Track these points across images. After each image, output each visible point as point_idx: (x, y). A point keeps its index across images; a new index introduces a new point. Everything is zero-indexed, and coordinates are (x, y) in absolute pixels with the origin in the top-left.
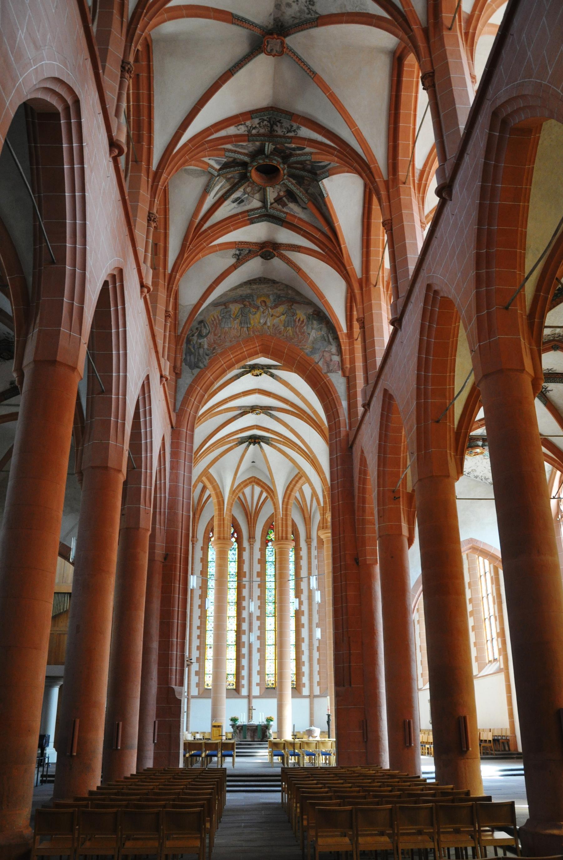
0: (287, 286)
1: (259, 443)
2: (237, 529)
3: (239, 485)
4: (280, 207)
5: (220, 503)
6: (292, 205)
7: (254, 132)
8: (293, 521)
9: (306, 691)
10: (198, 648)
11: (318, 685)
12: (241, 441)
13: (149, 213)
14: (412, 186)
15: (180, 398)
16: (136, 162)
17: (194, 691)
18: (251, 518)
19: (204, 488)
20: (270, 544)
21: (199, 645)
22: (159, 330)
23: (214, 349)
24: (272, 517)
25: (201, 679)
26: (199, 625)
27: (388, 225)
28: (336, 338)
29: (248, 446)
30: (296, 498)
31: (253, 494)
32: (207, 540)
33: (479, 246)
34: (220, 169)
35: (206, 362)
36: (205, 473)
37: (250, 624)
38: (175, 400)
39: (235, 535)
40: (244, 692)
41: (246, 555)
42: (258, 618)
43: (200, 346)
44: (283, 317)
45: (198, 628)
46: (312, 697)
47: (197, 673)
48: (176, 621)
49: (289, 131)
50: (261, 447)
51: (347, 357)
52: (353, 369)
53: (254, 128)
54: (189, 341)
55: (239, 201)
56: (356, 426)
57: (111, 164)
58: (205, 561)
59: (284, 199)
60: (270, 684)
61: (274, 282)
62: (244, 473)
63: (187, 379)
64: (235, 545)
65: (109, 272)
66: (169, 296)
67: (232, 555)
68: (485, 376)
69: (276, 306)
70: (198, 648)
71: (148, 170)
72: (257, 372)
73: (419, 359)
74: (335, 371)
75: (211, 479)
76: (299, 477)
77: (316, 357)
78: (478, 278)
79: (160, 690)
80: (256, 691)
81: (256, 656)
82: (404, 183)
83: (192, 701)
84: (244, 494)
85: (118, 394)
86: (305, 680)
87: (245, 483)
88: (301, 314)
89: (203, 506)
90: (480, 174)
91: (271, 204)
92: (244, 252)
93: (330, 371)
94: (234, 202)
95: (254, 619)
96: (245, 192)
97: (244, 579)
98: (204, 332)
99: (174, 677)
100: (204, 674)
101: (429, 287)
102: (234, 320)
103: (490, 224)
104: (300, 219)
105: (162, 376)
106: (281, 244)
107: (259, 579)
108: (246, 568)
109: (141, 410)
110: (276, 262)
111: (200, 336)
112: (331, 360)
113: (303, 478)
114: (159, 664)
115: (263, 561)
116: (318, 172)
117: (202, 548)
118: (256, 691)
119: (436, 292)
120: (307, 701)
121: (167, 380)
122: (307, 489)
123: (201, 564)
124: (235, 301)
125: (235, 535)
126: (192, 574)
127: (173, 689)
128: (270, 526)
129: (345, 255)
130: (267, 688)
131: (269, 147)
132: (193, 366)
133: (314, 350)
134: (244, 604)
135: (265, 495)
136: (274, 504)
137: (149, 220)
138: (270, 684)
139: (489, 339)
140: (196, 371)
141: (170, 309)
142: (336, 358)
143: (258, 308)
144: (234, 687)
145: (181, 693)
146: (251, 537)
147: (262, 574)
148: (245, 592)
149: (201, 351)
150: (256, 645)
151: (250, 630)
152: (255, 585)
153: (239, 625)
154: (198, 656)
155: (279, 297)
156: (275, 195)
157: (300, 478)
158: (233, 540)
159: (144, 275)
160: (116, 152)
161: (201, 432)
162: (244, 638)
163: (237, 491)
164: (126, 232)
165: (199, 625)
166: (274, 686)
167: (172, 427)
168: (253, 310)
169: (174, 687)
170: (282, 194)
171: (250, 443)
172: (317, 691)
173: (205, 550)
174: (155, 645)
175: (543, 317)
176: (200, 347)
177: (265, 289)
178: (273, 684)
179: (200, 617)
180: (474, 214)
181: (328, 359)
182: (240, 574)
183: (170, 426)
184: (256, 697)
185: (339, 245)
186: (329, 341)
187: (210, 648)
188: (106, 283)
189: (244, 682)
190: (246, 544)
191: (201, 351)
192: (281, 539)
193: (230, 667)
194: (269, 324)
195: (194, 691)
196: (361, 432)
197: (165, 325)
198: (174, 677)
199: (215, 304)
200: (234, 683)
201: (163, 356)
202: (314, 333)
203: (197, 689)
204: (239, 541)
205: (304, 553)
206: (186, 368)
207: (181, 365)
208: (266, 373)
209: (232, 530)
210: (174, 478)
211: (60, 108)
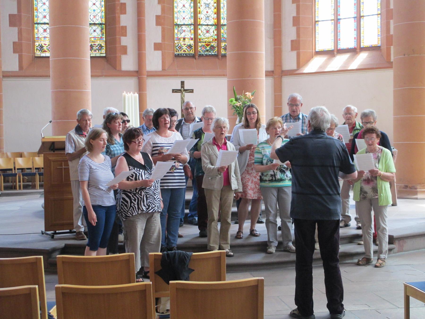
11: (293, 49)
25: (24, 34)
40: (128, 63)
60: (184, 48)
80: (154, 61)
100: (32, 24)
118: (154, 61)
130: (178, 56)
138: (184, 48)
144: (103, 52)
166: (192, 52)
172: (289, 61)
178: (190, 46)
189: (128, 41)
200: (103, 44)
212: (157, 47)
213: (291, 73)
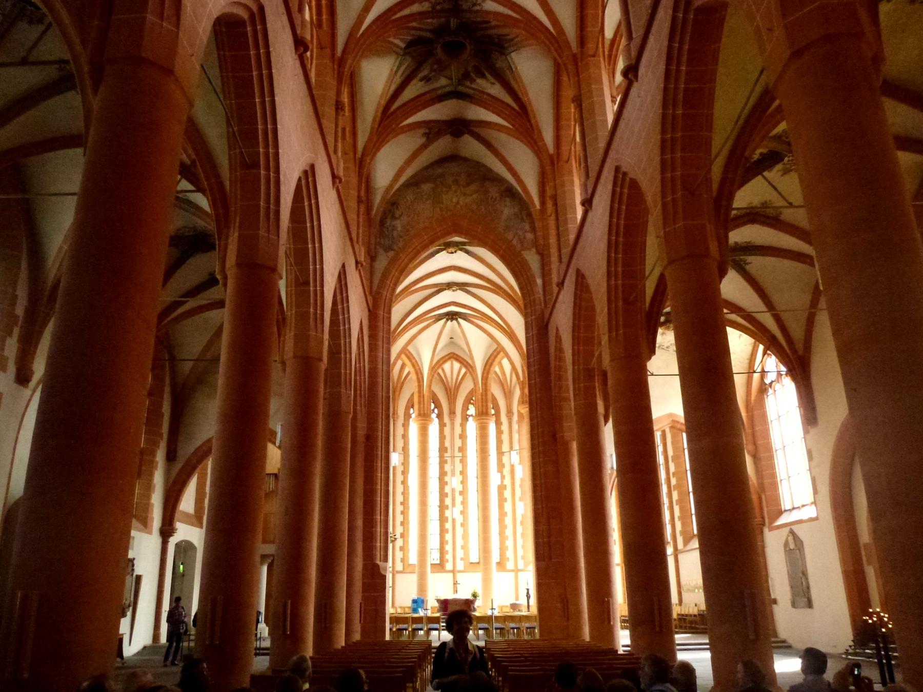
0: (478, 162)
1: (456, 319)
2: (438, 405)
3: (438, 362)
4: (468, 83)
5: (420, 380)
6: (480, 81)
7: (438, 7)
8: (493, 395)
9: (510, 565)
12: (439, 318)
13: (337, 101)
14: (602, 59)
15: (376, 282)
16: (322, 48)
17: (399, 567)
18: (451, 393)
19: (403, 366)
20: (470, 419)
22: (352, 216)
23: (408, 230)
24: (471, 393)
27: (578, 101)
28: (530, 215)
29: (446, 323)
30: (496, 373)
31: (452, 369)
32: (407, 416)
33: (663, 131)
34: (406, 48)
35: (401, 245)
36: (404, 351)
37: (453, 499)
38: (371, 283)
39: (436, 411)
40: (449, 566)
41: (447, 431)
42: (461, 493)
43: (394, 228)
44: (475, 196)
45: (402, 504)
46: (516, 571)
47: (401, 549)
48: (379, 499)
49: (474, 5)
50: (459, 323)
51: (539, 234)
52: (547, 246)
53: (438, 4)
54: (382, 223)
55: (427, 79)
56: (551, 304)
57: (298, 63)
58: (405, 437)
59: (473, 75)
61: (465, 159)
62: (442, 349)
63: (382, 262)
64: (436, 421)
65: (301, 169)
66: (360, 182)
67: (434, 428)
68: (670, 263)
69: (468, 184)
70: (402, 524)
71: (333, 55)
72: (451, 250)
73: (609, 241)
74: (529, 249)
75: (410, 357)
76: (497, 352)
77: (510, 236)
78: (663, 163)
79: (365, 566)
80: (460, 565)
81: (459, 531)
82: (594, 56)
83: (398, 576)
84: (443, 370)
85: (315, 286)
86: (510, 554)
87: (444, 360)
88: (494, 192)
89: (403, 383)
90: (664, 57)
91: (459, 81)
92: (433, 131)
93: (525, 249)
94: (421, 80)
95: (457, 494)
96: (432, 70)
97: (446, 455)
98: (398, 213)
99: (378, 554)
101: (617, 169)
102: (427, 199)
103: (674, 110)
104: (489, 95)
105: (357, 262)
106: (471, 121)
107: (460, 454)
108: (447, 444)
109: (339, 298)
110: (467, 138)
111: (394, 218)
112: (525, 238)
113: (502, 354)
114: (364, 541)
115: (463, 436)
116: (506, 45)
117: (403, 425)
118: (460, 565)
119: (625, 174)
120: (513, 574)
121: (362, 265)
122: (506, 363)
124: (426, 180)
125: (436, 411)
126: (394, 451)
127: (378, 566)
128: (468, 402)
129: (536, 131)
131: (453, 22)
132: (387, 249)
133: (507, 228)
134: (447, 479)
135: (464, 370)
136: (474, 380)
137: (337, 109)
139: (675, 224)
140: (391, 254)
141: (363, 193)
142: (530, 236)
143: (450, 187)
144: (438, 562)
145: (385, 569)
146: (452, 413)
147: (462, 449)
148: (447, 468)
149: (395, 234)
150: (459, 519)
151: (454, 505)
152: (457, 460)
153: (442, 501)
155: (469, 175)
156: (462, 71)
157: (498, 353)
158: (434, 416)
159: (335, 166)
160: (302, 49)
161: (398, 310)
162: (448, 513)
163: (436, 367)
164: (316, 126)
167: (369, 310)
168: (444, 189)
169: (378, 562)
170: (470, 69)
171: (448, 320)
172: (521, 565)
173: (406, 426)
174: (360, 523)
175: (731, 197)
176: (393, 230)
177: (454, 168)
180: (659, 97)
181: (522, 237)
182: (442, 449)
183: (367, 310)
184: (460, 572)
185: (529, 121)
186: (523, 218)
188: (300, 179)
189: (449, 557)
190: (446, 419)
191: (395, 234)
192: (482, 414)
193: (433, 542)
194: (461, 203)
195: (399, 567)
196: (555, 311)
197: (358, 211)
198: (378, 553)
199: (408, 185)
201: (358, 242)
202: (507, 210)
204: (440, 416)
205: (505, 427)
206: (381, 251)
207: (375, 248)
208: (461, 250)
209: (433, 406)
210: (373, 359)
211: (244, 14)
212: (462, 559)
213: (521, 570)
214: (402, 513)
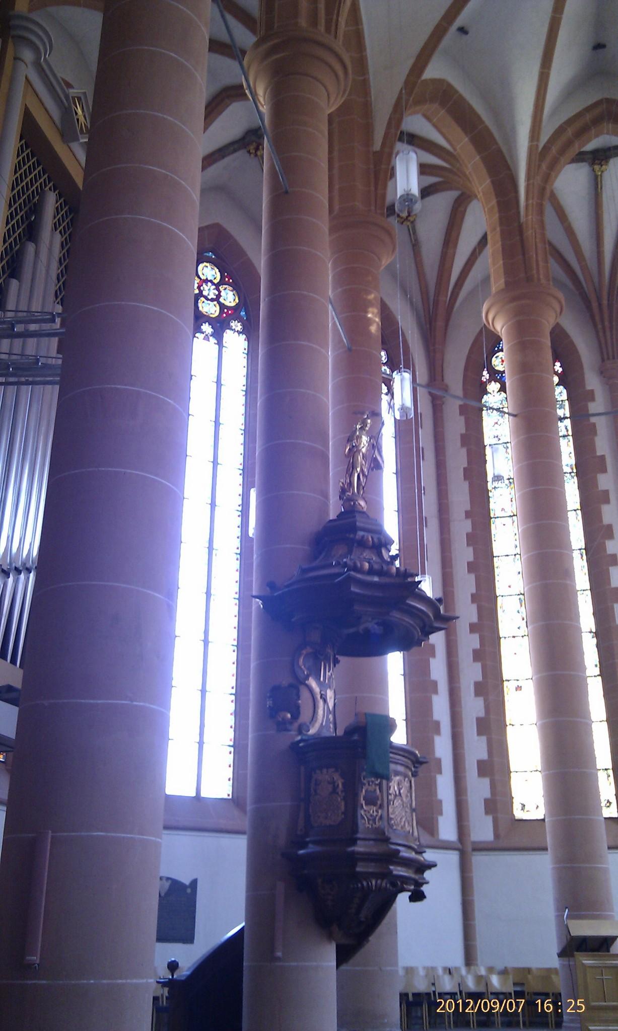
10: (480, 689)
21: (480, 678)
26: (475, 619)
45: (473, 628)
47: (484, 769)
70: (480, 689)
123: (464, 451)
154: (482, 714)
165: (475, 619)
179: (474, 598)
187: (519, 688)
203: (489, 819)
214: (478, 655)
